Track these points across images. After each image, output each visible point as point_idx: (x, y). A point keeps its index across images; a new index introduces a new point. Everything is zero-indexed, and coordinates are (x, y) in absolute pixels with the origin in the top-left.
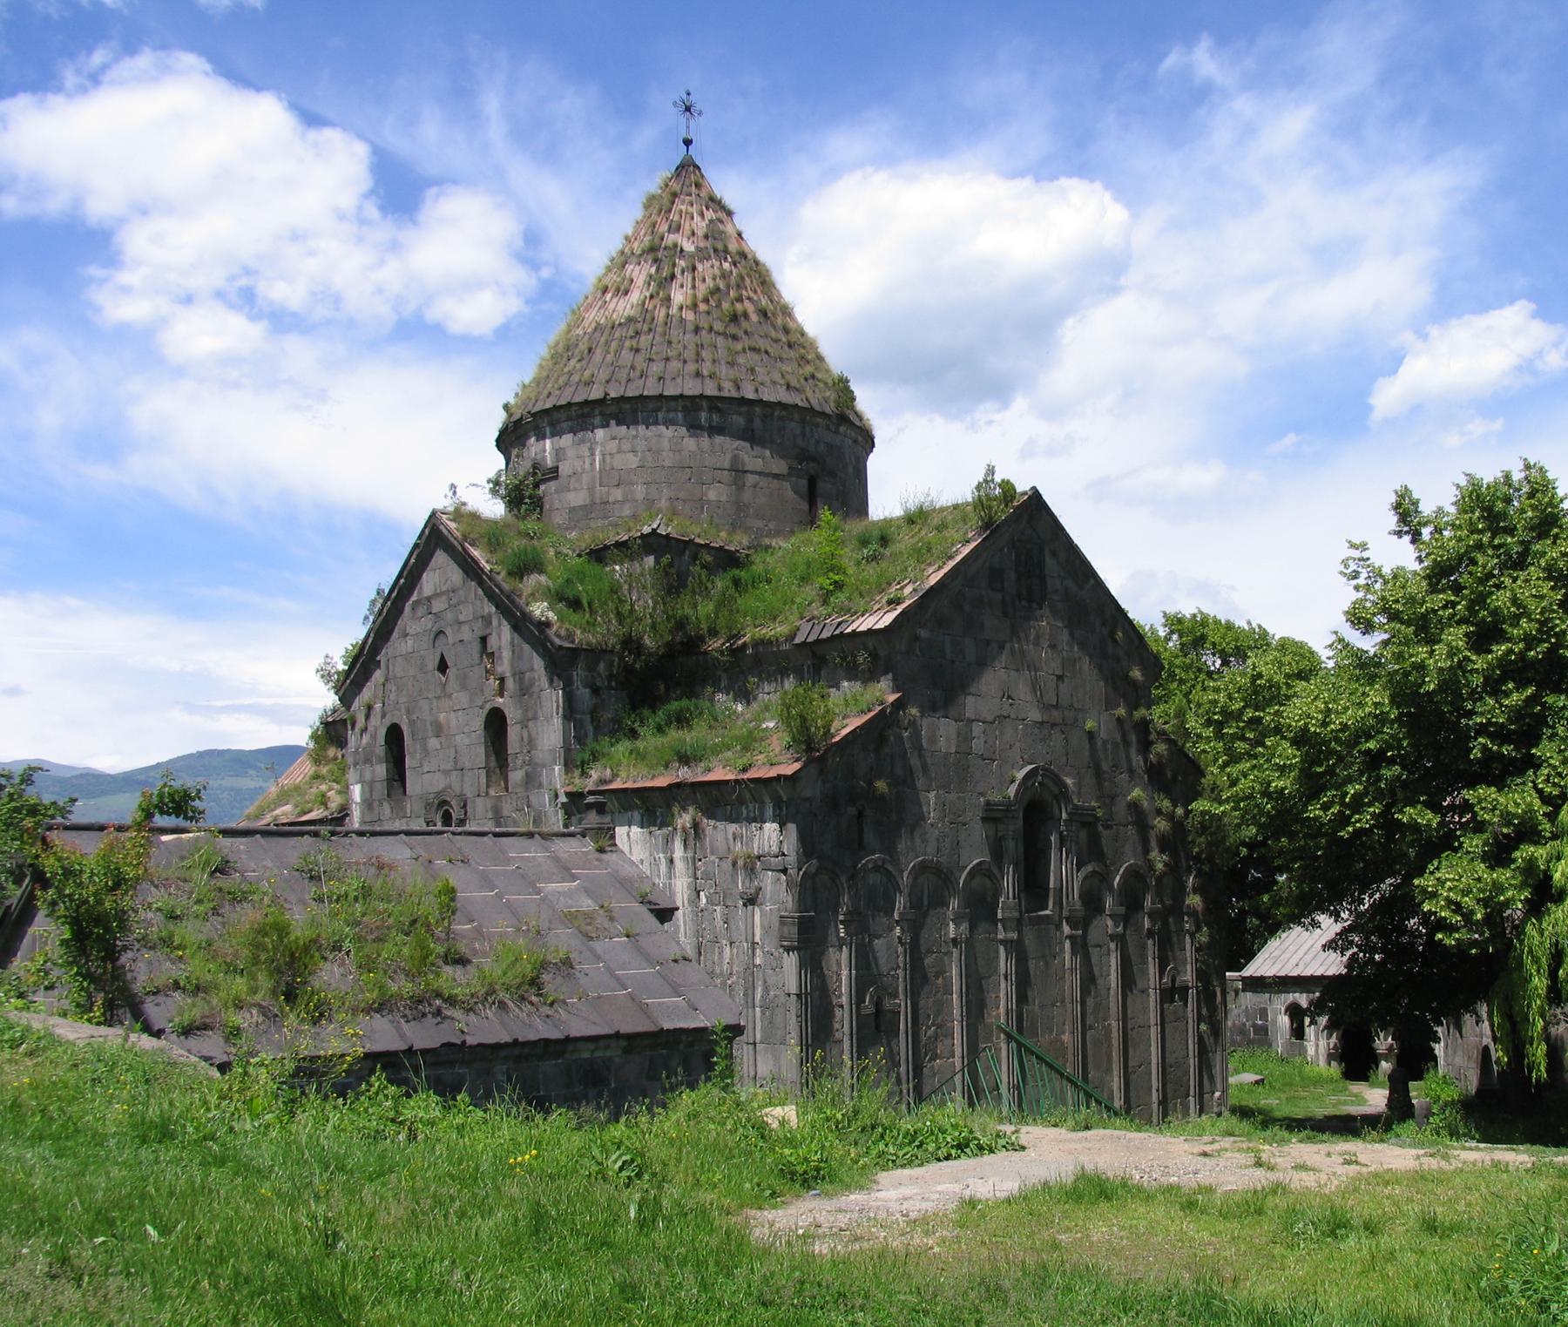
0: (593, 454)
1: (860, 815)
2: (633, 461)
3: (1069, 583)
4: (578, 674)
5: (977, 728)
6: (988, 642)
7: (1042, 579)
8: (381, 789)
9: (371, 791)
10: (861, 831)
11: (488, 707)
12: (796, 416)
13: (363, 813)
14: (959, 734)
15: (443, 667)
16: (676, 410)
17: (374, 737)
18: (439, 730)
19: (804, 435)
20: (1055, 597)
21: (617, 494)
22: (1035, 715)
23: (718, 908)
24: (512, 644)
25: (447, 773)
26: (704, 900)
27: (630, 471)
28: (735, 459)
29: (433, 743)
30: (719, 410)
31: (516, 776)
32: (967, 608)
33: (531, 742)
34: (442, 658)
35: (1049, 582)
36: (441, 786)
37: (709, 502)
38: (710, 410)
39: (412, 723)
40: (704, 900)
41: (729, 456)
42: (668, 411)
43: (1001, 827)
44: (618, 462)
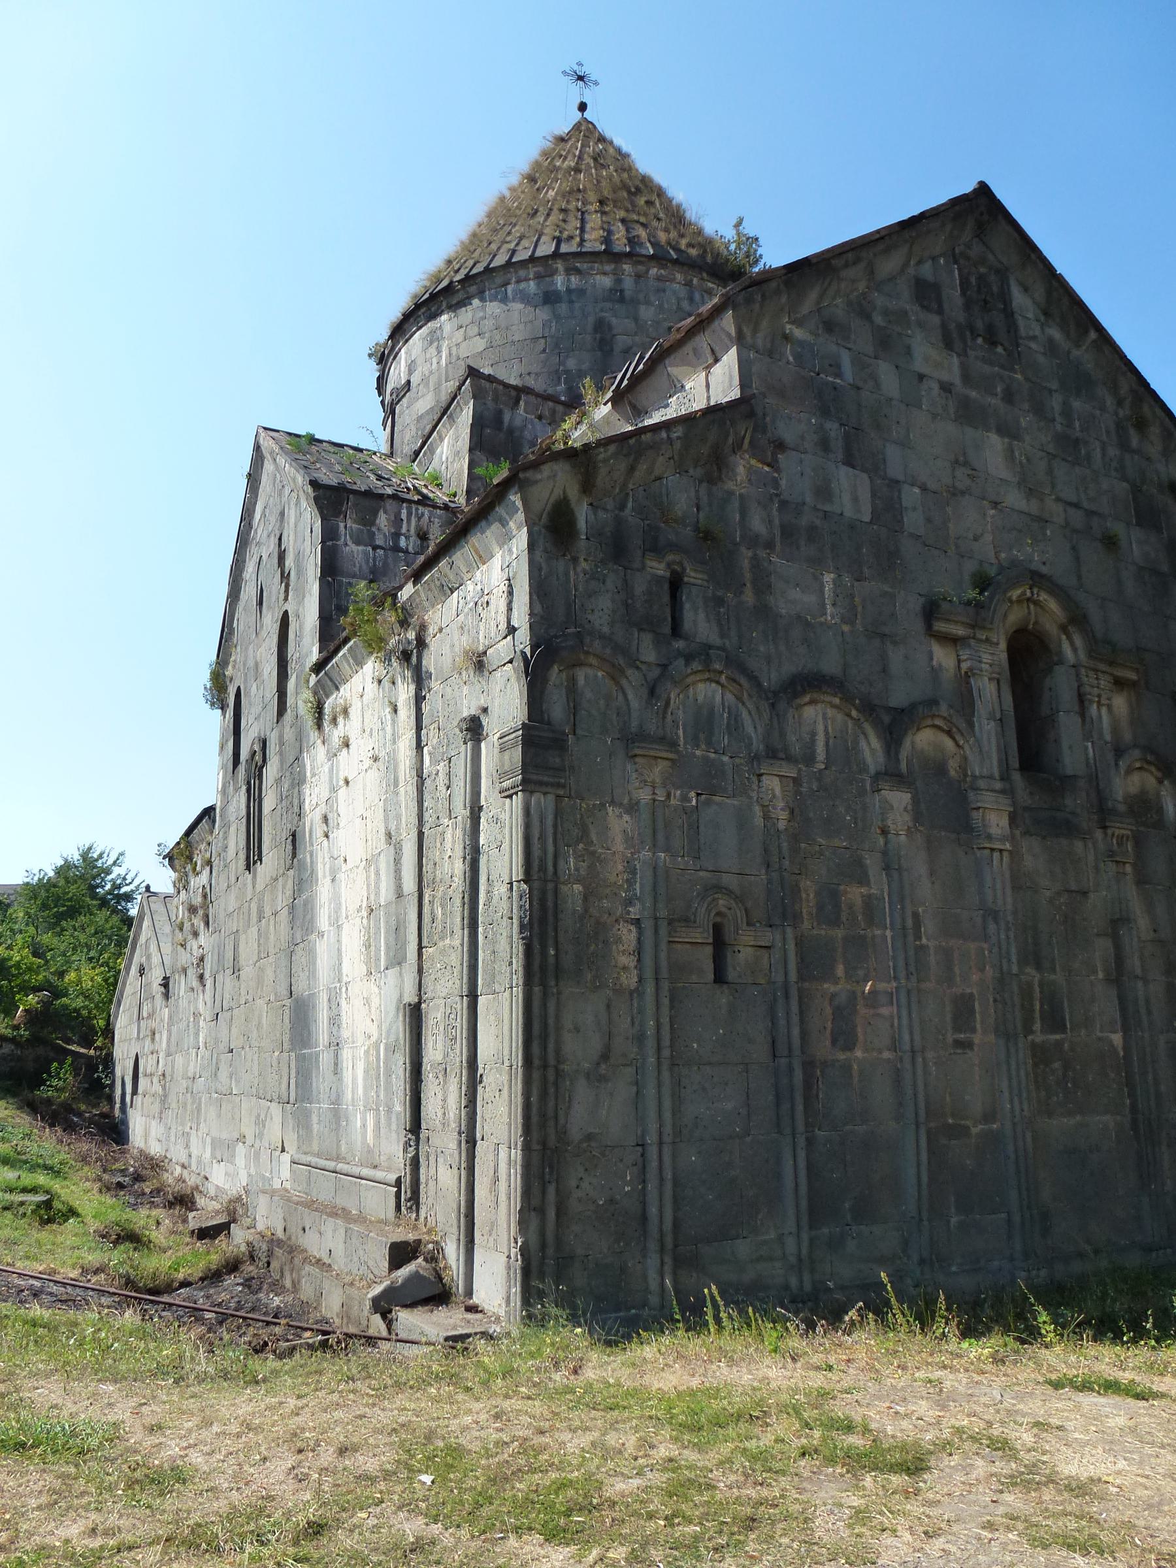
0: (439, 352)
1: (675, 584)
4: (347, 526)
5: (911, 495)
6: (921, 377)
7: (1009, 313)
12: (679, 276)
14: (874, 494)
16: (527, 280)
19: (691, 299)
20: (1033, 345)
30: (578, 271)
32: (878, 319)
35: (1021, 323)
37: (567, 372)
38: (569, 271)
41: (591, 320)
42: (518, 281)
43: (965, 654)
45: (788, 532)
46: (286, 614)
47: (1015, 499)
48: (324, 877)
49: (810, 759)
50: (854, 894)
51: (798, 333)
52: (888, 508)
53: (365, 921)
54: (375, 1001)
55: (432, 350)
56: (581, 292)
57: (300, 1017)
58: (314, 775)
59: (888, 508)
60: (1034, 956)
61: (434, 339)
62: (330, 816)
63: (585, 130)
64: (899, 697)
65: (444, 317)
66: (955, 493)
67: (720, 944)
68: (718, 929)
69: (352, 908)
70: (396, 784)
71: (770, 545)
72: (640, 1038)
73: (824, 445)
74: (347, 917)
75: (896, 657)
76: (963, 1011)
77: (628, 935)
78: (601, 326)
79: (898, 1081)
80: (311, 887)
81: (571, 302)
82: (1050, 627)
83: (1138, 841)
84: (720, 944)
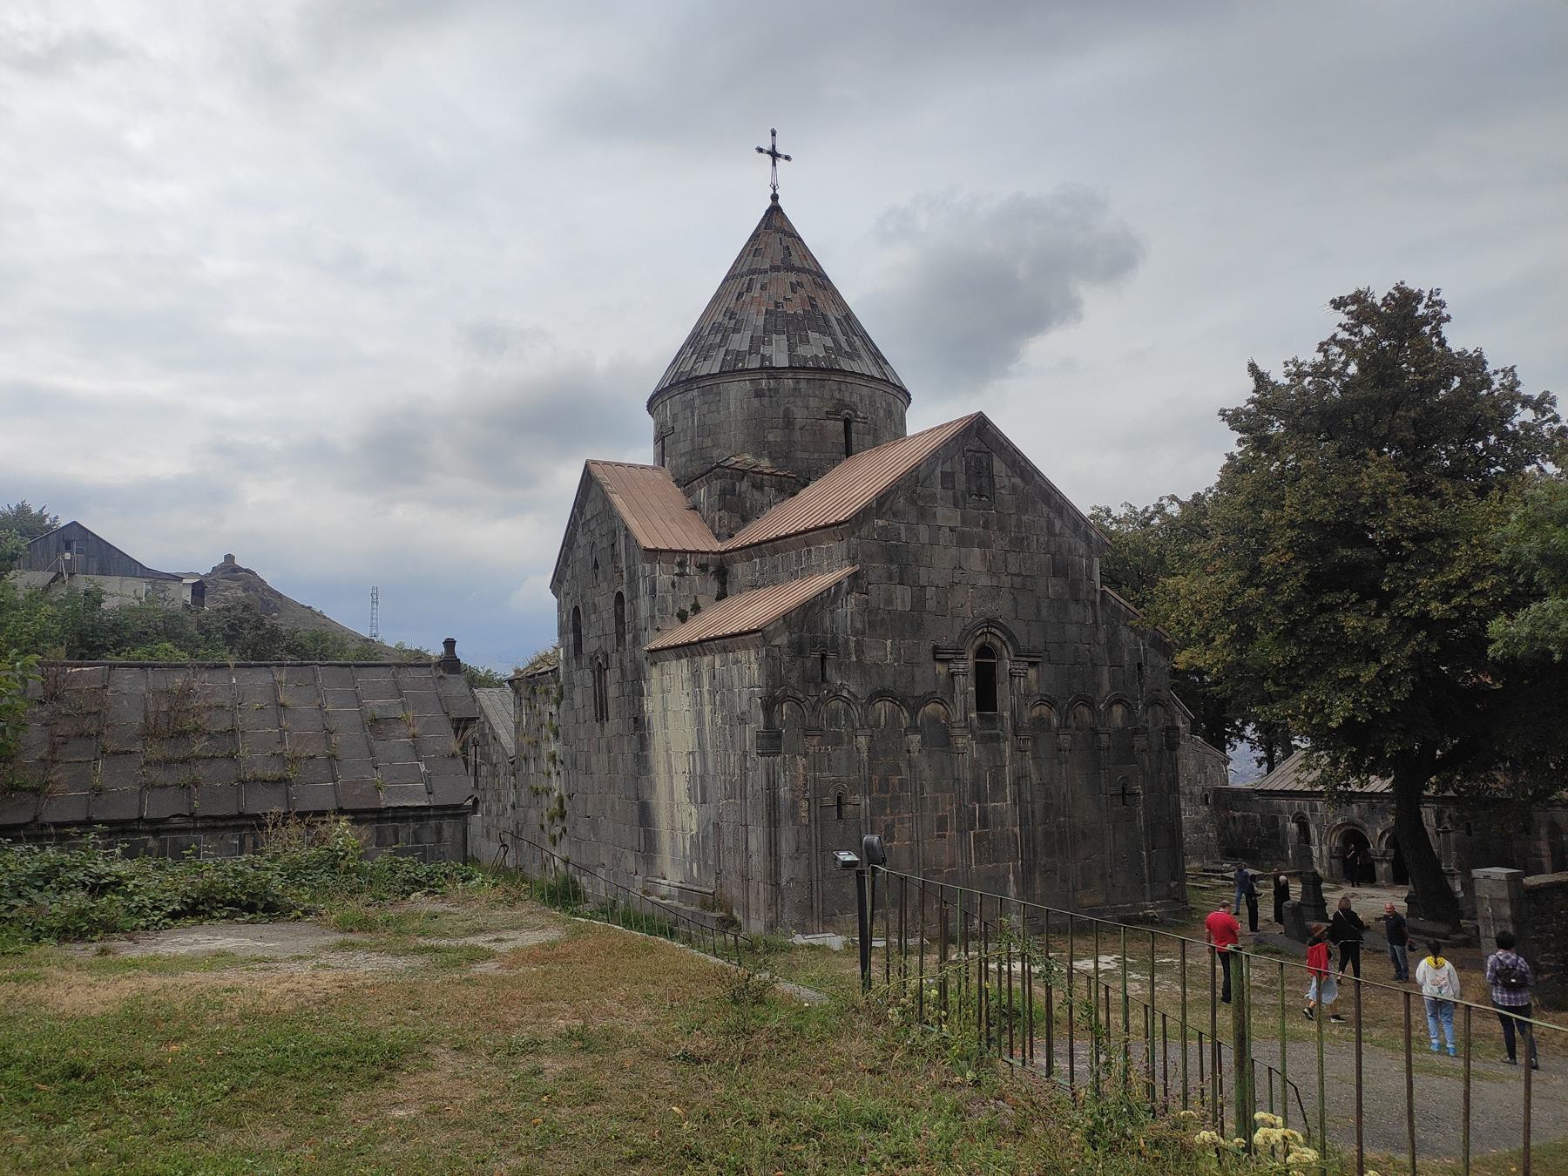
1: (823, 657)
3: (1018, 481)
7: (991, 477)
8: (571, 649)
10: (823, 668)
21: (708, 442)
22: (985, 581)
28: (787, 410)
31: (629, 637)
32: (920, 503)
35: (997, 480)
45: (872, 625)
46: (620, 595)
47: (985, 581)
49: (878, 725)
50: (895, 780)
51: (880, 523)
52: (919, 602)
54: (695, 816)
56: (776, 391)
57: (645, 815)
59: (919, 602)
60: (978, 796)
61: (689, 406)
63: (775, 211)
64: (919, 692)
65: (695, 393)
66: (953, 584)
67: (840, 803)
68: (839, 798)
69: (680, 771)
71: (863, 633)
72: (810, 843)
73: (890, 578)
75: (918, 672)
76: (942, 824)
77: (805, 804)
78: (787, 410)
79: (912, 852)
82: (998, 644)
83: (1035, 740)
84: (840, 803)
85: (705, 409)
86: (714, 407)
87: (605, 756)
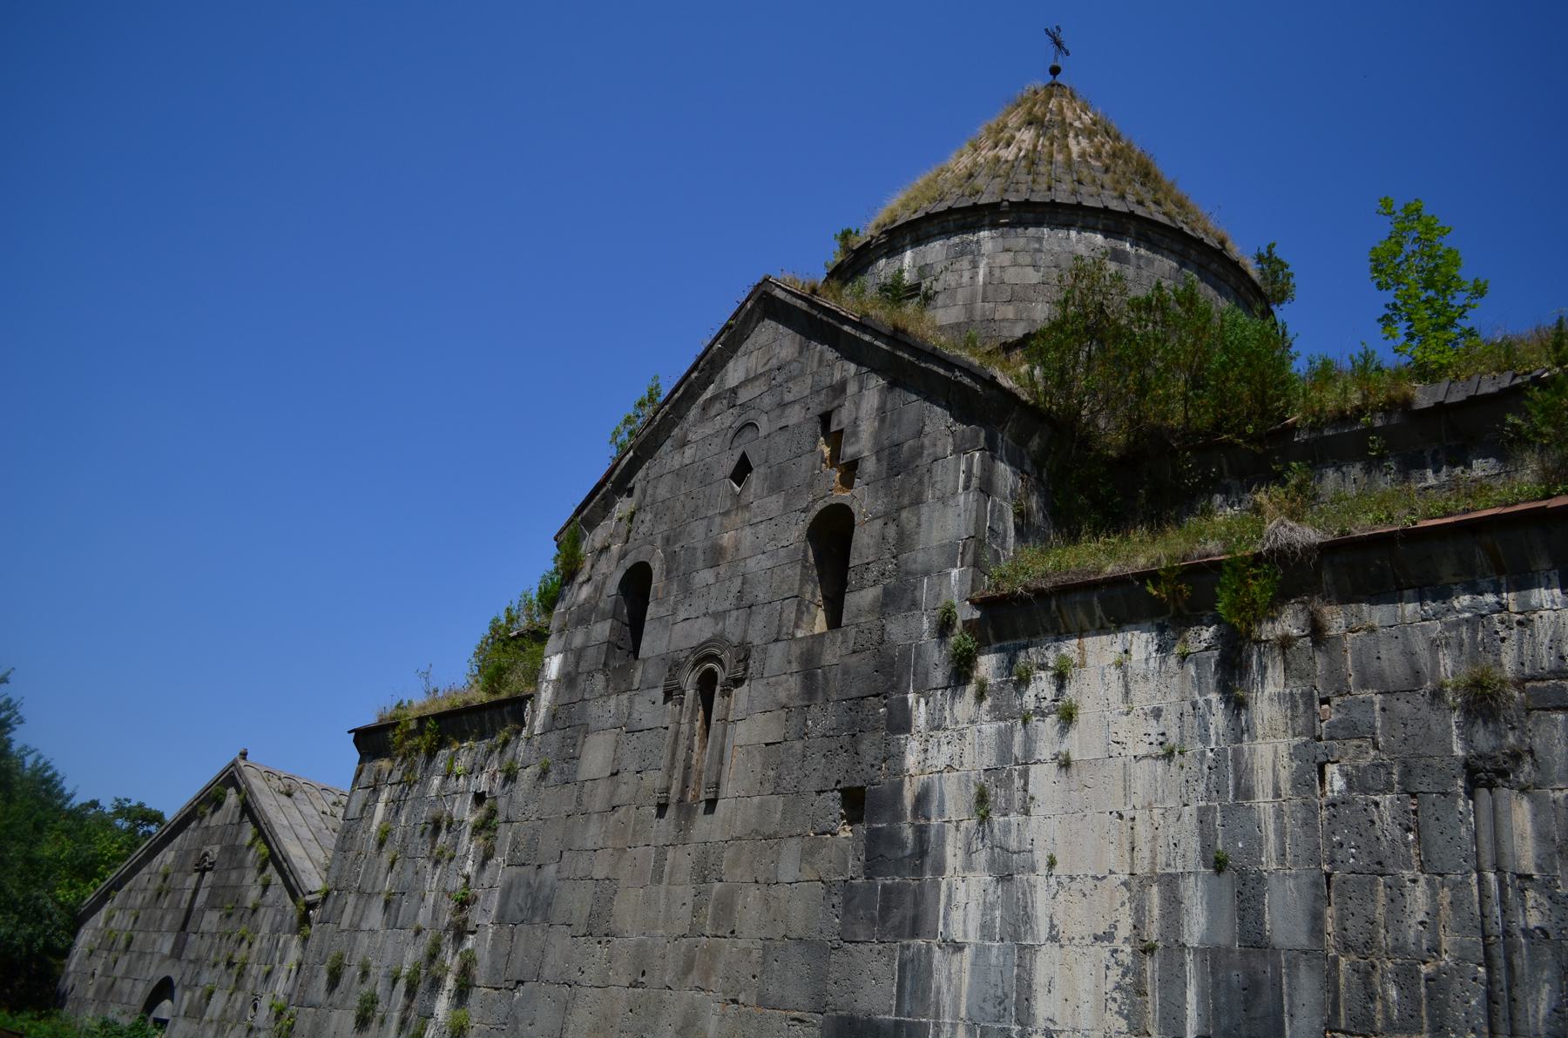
2: (1033, 277)
9: (577, 665)
11: (819, 506)
13: (556, 693)
15: (742, 471)
17: (599, 589)
18: (716, 556)
21: (1009, 312)
23: (1386, 800)
24: (882, 410)
25: (719, 616)
26: (1336, 781)
27: (1026, 287)
29: (705, 576)
33: (904, 542)
34: (744, 457)
36: (707, 635)
39: (671, 558)
40: (1336, 781)
44: (1011, 276)
48: (969, 866)
53: (1126, 956)
55: (965, 263)
58: (936, 725)
62: (997, 796)
65: (984, 234)
70: (1244, 792)
74: (1053, 938)
80: (918, 871)
81: (1139, 267)
85: (1006, 259)
86: (1025, 259)
87: (685, 892)
